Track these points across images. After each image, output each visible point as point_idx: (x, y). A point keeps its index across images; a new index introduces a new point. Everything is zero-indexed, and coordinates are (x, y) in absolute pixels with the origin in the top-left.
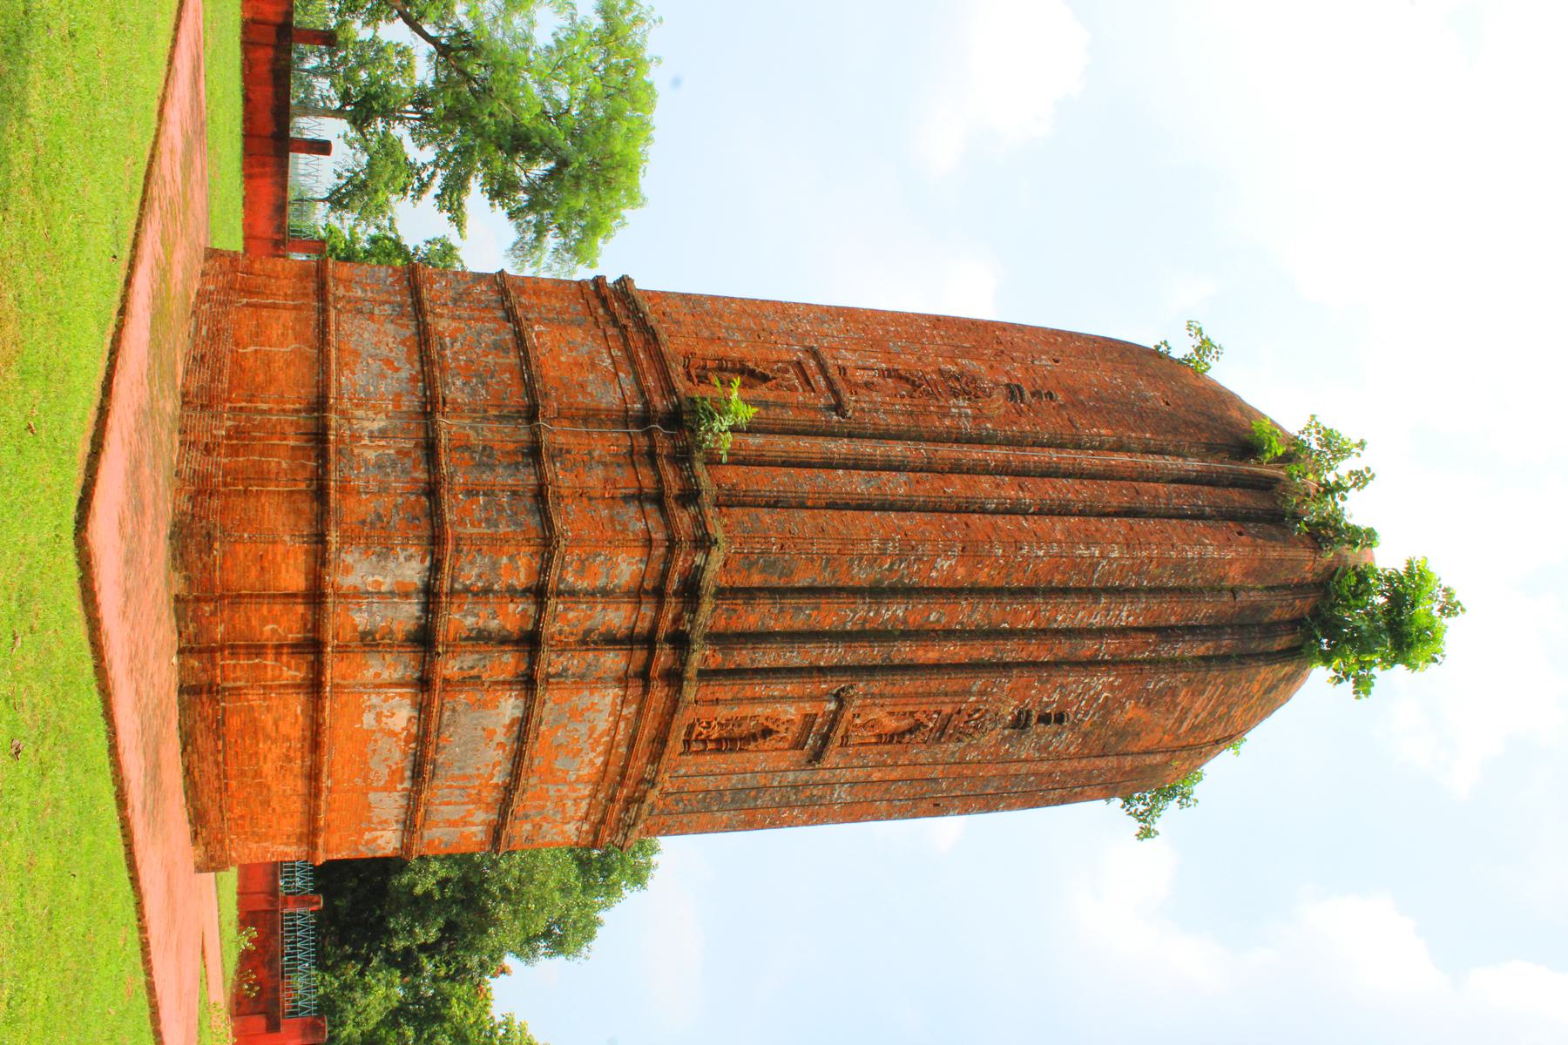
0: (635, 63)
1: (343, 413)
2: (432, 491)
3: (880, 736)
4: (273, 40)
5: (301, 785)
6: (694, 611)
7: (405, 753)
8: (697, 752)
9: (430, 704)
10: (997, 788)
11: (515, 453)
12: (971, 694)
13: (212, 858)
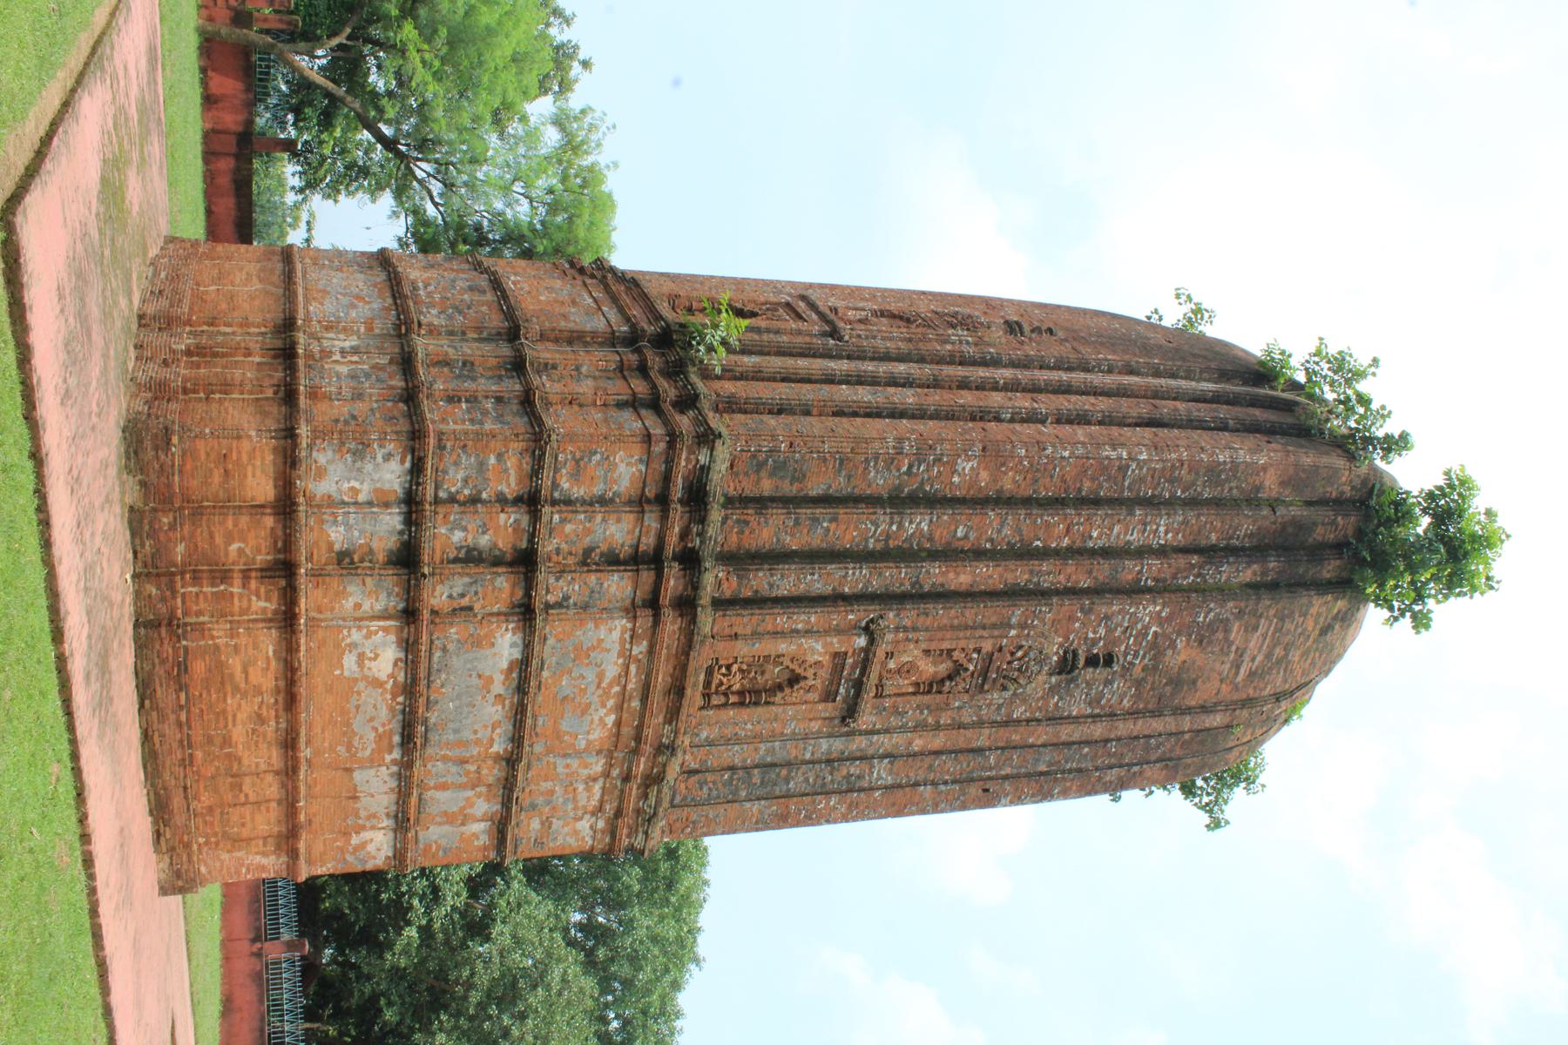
0: (591, 177)
1: (314, 336)
3: (917, 684)
4: (234, 150)
5: (276, 757)
6: (702, 521)
7: (392, 709)
8: (718, 707)
9: (417, 642)
10: (1050, 764)
11: (499, 367)
12: (1011, 627)
13: (178, 875)
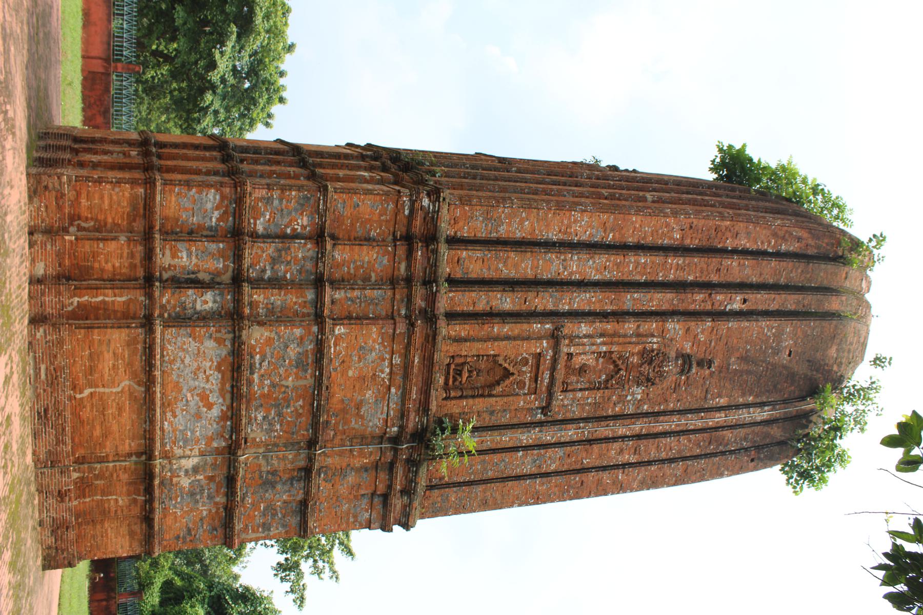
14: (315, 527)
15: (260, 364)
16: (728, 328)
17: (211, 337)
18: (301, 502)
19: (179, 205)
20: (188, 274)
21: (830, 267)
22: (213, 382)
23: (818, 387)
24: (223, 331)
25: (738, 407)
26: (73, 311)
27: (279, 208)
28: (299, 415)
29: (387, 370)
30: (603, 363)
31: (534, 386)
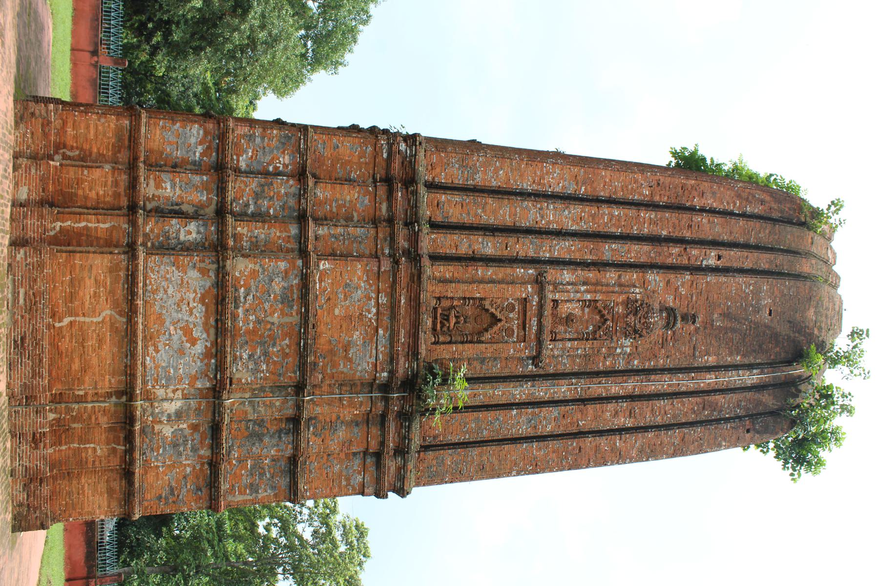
2: (214, 465)
14: (306, 491)
15: (245, 298)
16: (707, 282)
17: (194, 267)
18: (289, 458)
19: (164, 138)
20: (172, 205)
21: (796, 230)
22: (197, 315)
23: (802, 350)
24: (207, 261)
25: (727, 367)
26: (55, 236)
27: (261, 145)
28: (286, 355)
29: (374, 310)
30: (588, 313)
31: (522, 333)
